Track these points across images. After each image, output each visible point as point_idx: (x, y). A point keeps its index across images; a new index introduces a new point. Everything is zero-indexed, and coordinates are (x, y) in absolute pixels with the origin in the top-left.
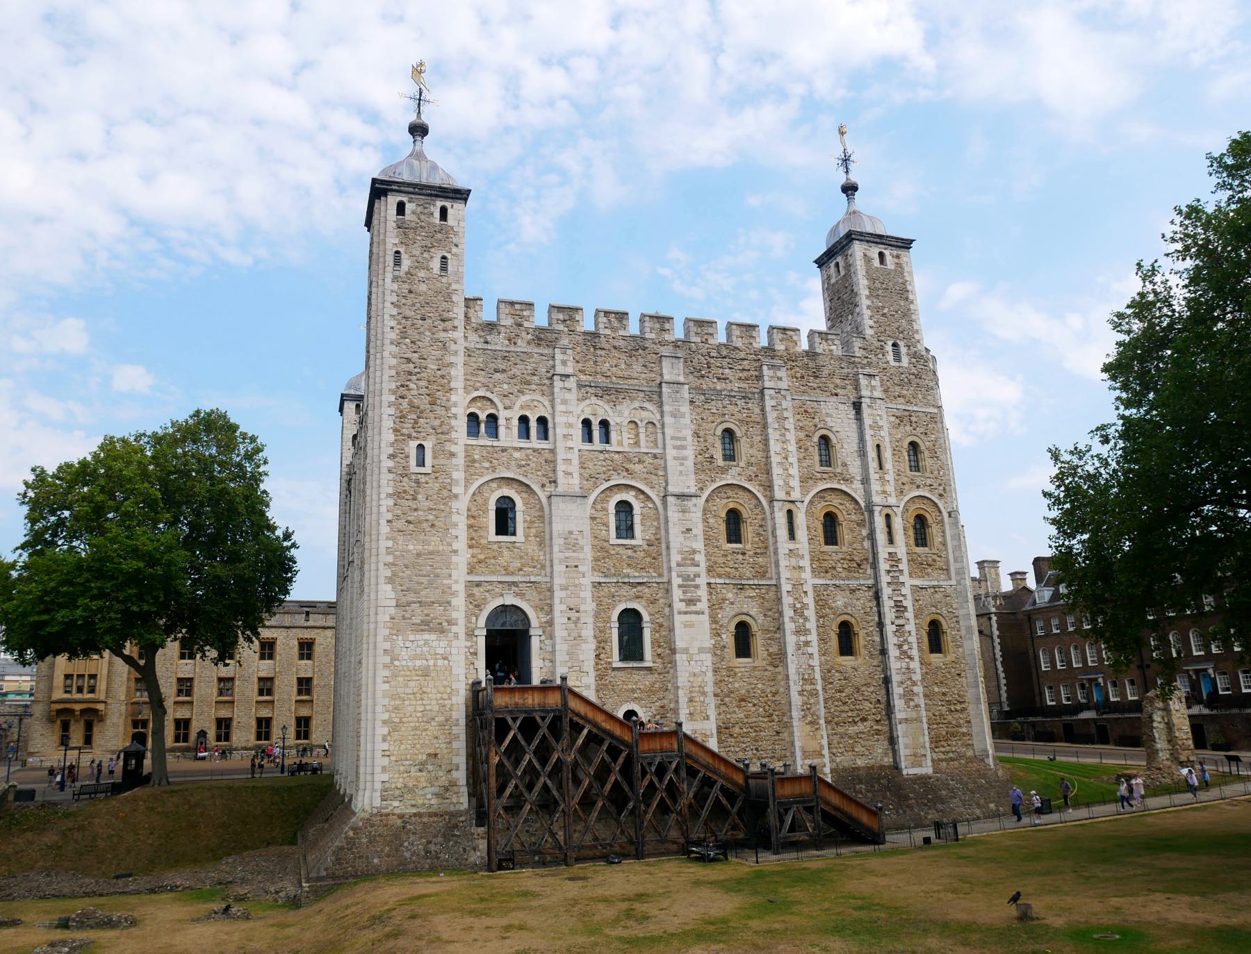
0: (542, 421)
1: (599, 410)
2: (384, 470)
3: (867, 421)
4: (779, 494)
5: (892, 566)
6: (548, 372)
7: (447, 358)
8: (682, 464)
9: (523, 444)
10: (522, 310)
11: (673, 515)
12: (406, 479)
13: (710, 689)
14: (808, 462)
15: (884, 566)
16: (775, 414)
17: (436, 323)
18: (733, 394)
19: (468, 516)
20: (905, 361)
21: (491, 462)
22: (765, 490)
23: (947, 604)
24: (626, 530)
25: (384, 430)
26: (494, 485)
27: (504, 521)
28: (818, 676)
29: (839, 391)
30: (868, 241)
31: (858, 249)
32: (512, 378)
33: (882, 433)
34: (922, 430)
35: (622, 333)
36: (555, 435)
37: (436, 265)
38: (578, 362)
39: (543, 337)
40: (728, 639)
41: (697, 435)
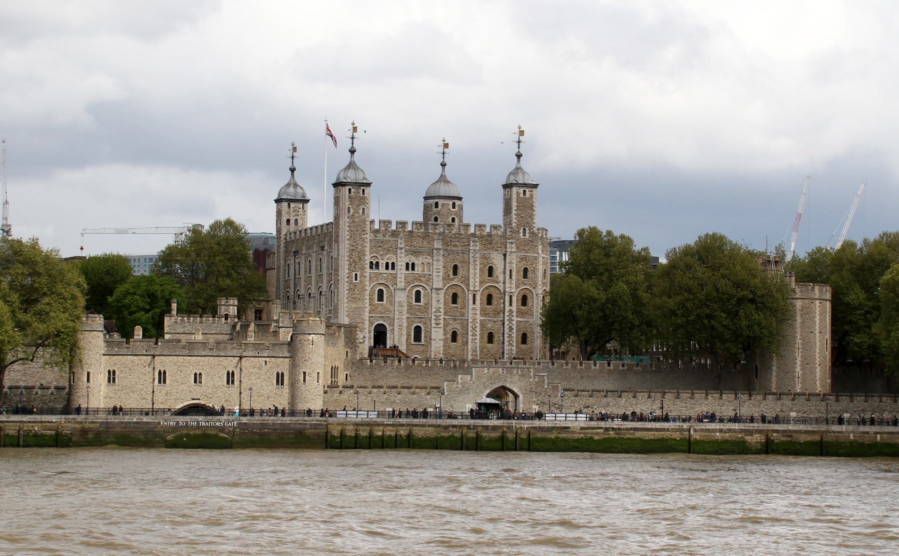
1: (412, 259)
3: (508, 261)
4: (471, 288)
9: (387, 271)
11: (434, 295)
13: (441, 352)
14: (483, 276)
15: (507, 314)
19: (370, 296)
24: (418, 300)
27: (381, 297)
28: (478, 350)
31: (515, 190)
37: (361, 211)
39: (394, 234)
40: (449, 336)
41: (444, 267)
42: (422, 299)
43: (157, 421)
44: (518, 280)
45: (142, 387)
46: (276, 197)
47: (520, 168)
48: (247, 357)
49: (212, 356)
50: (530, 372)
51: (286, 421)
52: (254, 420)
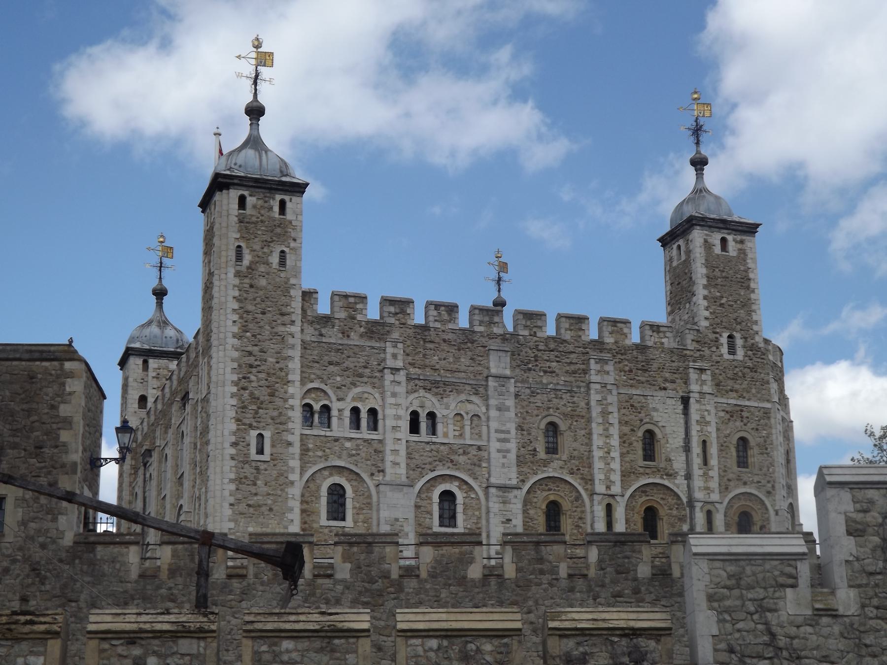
0: (373, 412)
2: (228, 457)
3: (694, 416)
4: (600, 488)
6: (379, 365)
7: (285, 351)
8: (504, 457)
10: (356, 303)
11: (495, 506)
12: (247, 466)
17: (275, 318)
18: (559, 387)
19: (302, 502)
20: (740, 354)
21: (324, 451)
22: (586, 483)
25: (227, 420)
26: (326, 473)
30: (710, 227)
31: (697, 236)
32: (347, 369)
33: (709, 429)
34: (754, 425)
35: (451, 326)
36: (385, 426)
37: (275, 259)
38: (408, 355)
39: (376, 330)
41: (520, 428)
42: (460, 518)
44: (724, 470)
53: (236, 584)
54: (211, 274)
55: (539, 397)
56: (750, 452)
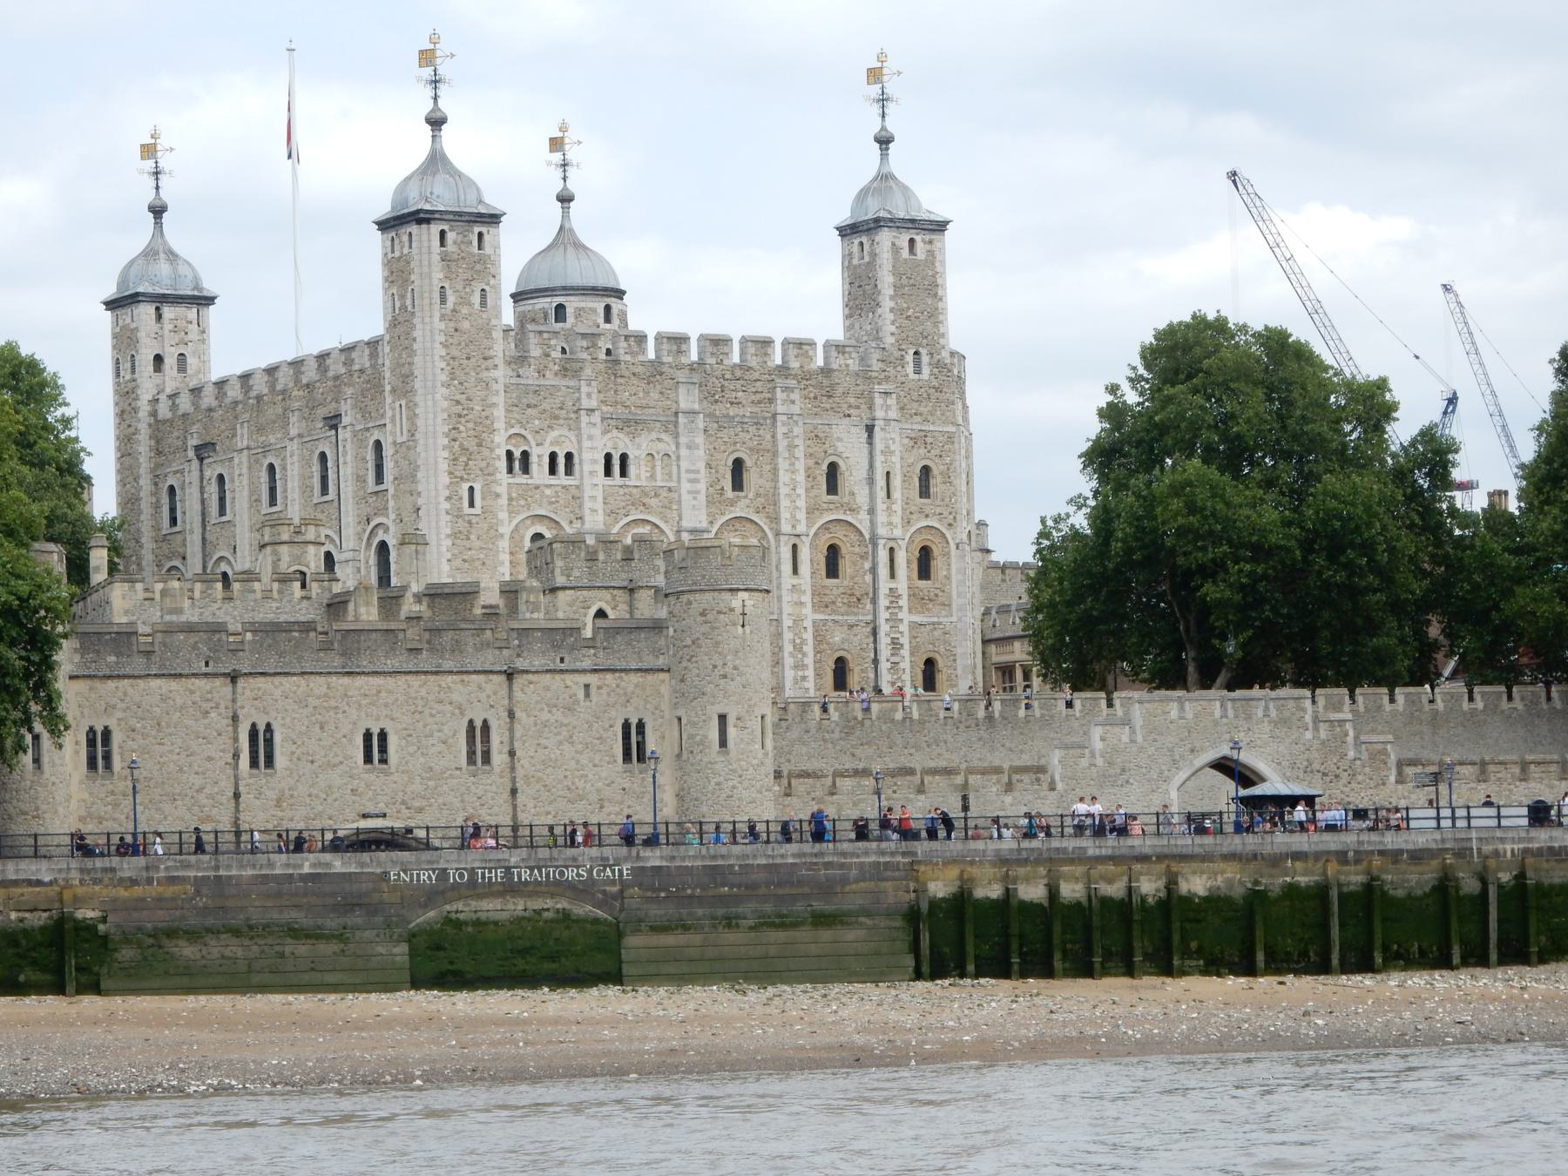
0: (569, 456)
2: (443, 512)
4: (786, 528)
5: (892, 602)
8: (695, 498)
9: (552, 480)
14: (815, 492)
15: (883, 602)
16: (785, 443)
18: (746, 420)
23: (945, 642)
26: (528, 522)
29: (852, 411)
31: (885, 237)
34: (937, 452)
35: (641, 358)
36: (581, 471)
37: (476, 299)
41: (709, 466)
43: (379, 871)
45: (198, 781)
46: (110, 290)
47: (893, 178)
48: (527, 672)
49: (417, 672)
50: (1304, 710)
51: (782, 856)
52: (683, 858)
53: (784, 724)
54: (404, 308)
55: (726, 431)
56: (932, 482)
